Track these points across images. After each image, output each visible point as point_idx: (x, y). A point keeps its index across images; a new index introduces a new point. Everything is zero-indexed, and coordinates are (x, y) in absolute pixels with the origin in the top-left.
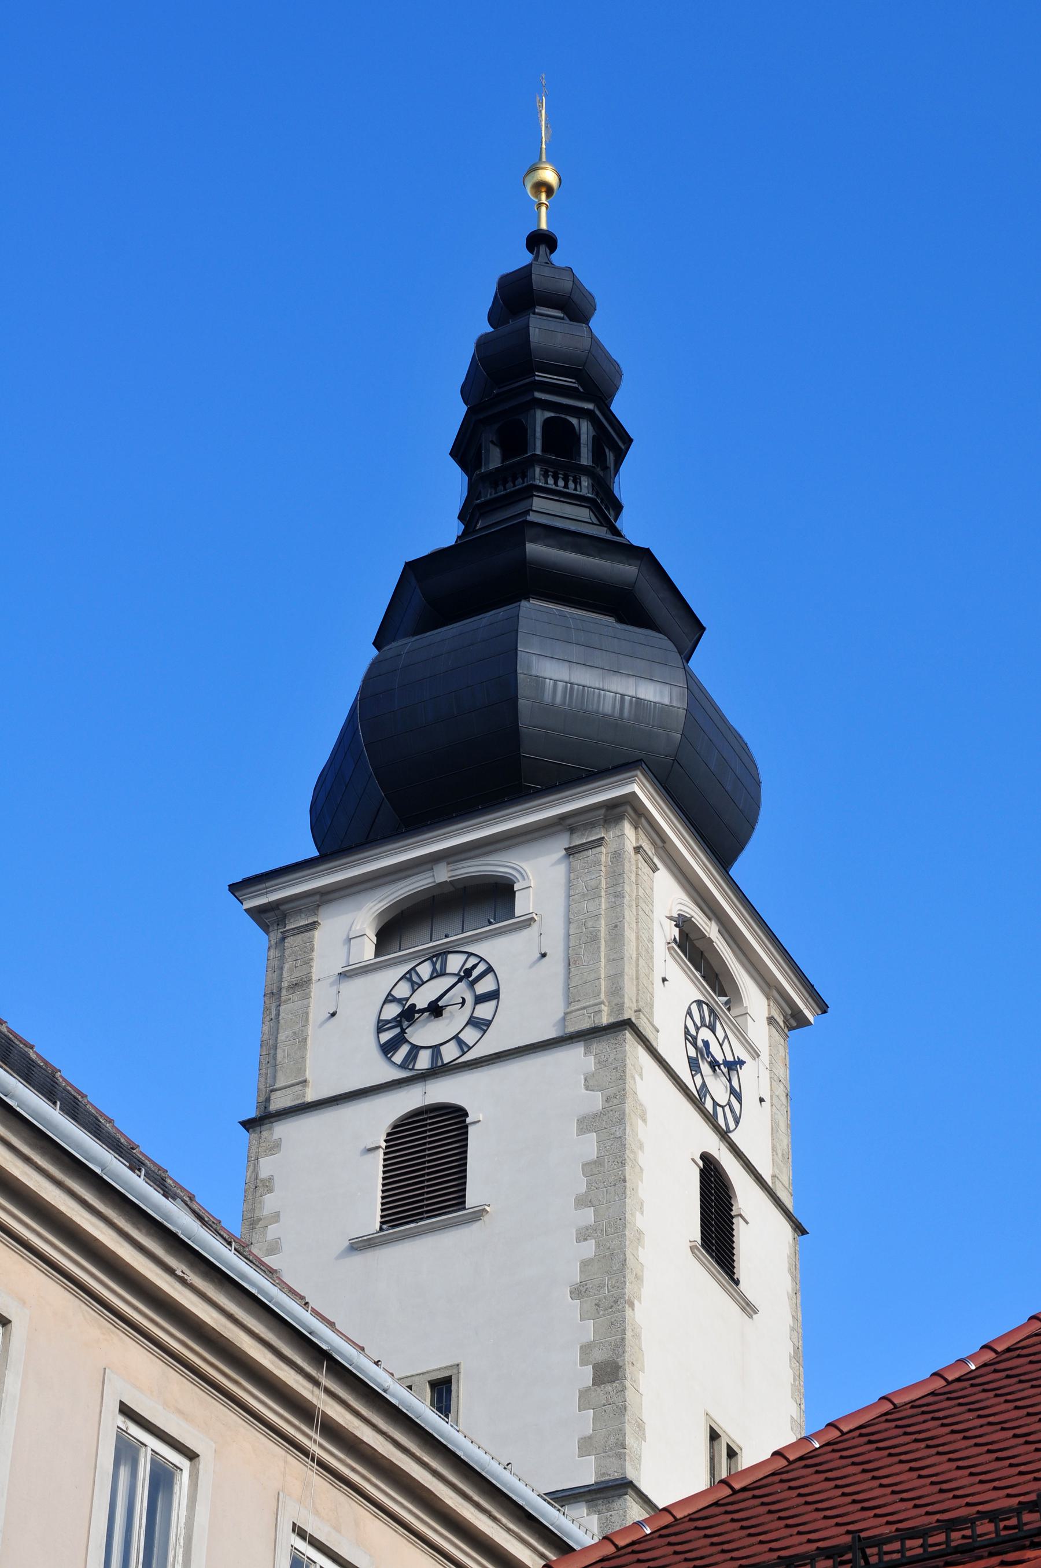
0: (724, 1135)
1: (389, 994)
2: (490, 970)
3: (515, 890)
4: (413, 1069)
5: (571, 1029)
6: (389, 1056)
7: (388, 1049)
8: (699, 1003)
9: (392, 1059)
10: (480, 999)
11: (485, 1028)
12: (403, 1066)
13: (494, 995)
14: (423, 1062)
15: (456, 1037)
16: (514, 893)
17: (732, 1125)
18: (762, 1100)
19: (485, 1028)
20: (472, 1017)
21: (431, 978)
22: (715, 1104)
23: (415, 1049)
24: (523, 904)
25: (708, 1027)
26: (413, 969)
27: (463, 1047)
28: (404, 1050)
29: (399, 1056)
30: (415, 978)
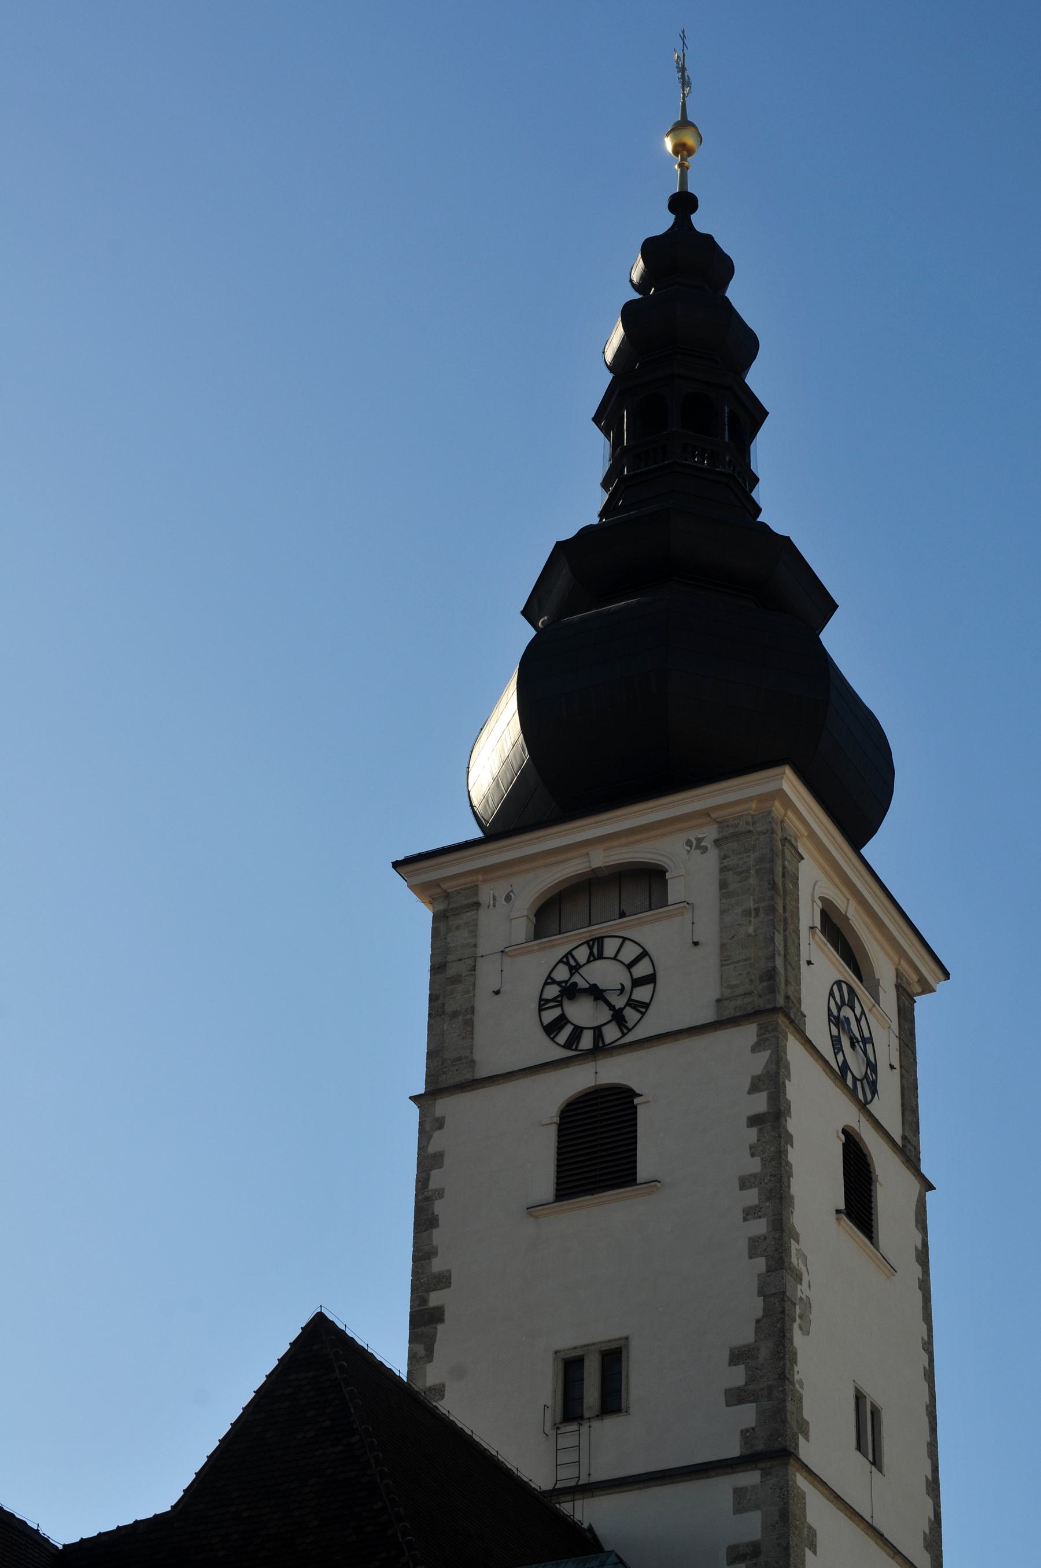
0: (863, 1106)
1: (549, 977)
2: (645, 954)
3: (667, 878)
4: (576, 1049)
5: (727, 1014)
6: (552, 1036)
7: (551, 1029)
8: (839, 983)
9: (556, 1040)
10: (637, 982)
11: (643, 1010)
12: (568, 1045)
13: (650, 979)
14: (586, 1041)
16: (667, 881)
17: (869, 1097)
18: (892, 1067)
19: (643, 1010)
20: (630, 999)
21: (588, 962)
22: (855, 1079)
23: (578, 1032)
24: (675, 891)
25: (848, 1005)
26: (570, 953)
28: (568, 1030)
29: (563, 1037)
30: (573, 963)
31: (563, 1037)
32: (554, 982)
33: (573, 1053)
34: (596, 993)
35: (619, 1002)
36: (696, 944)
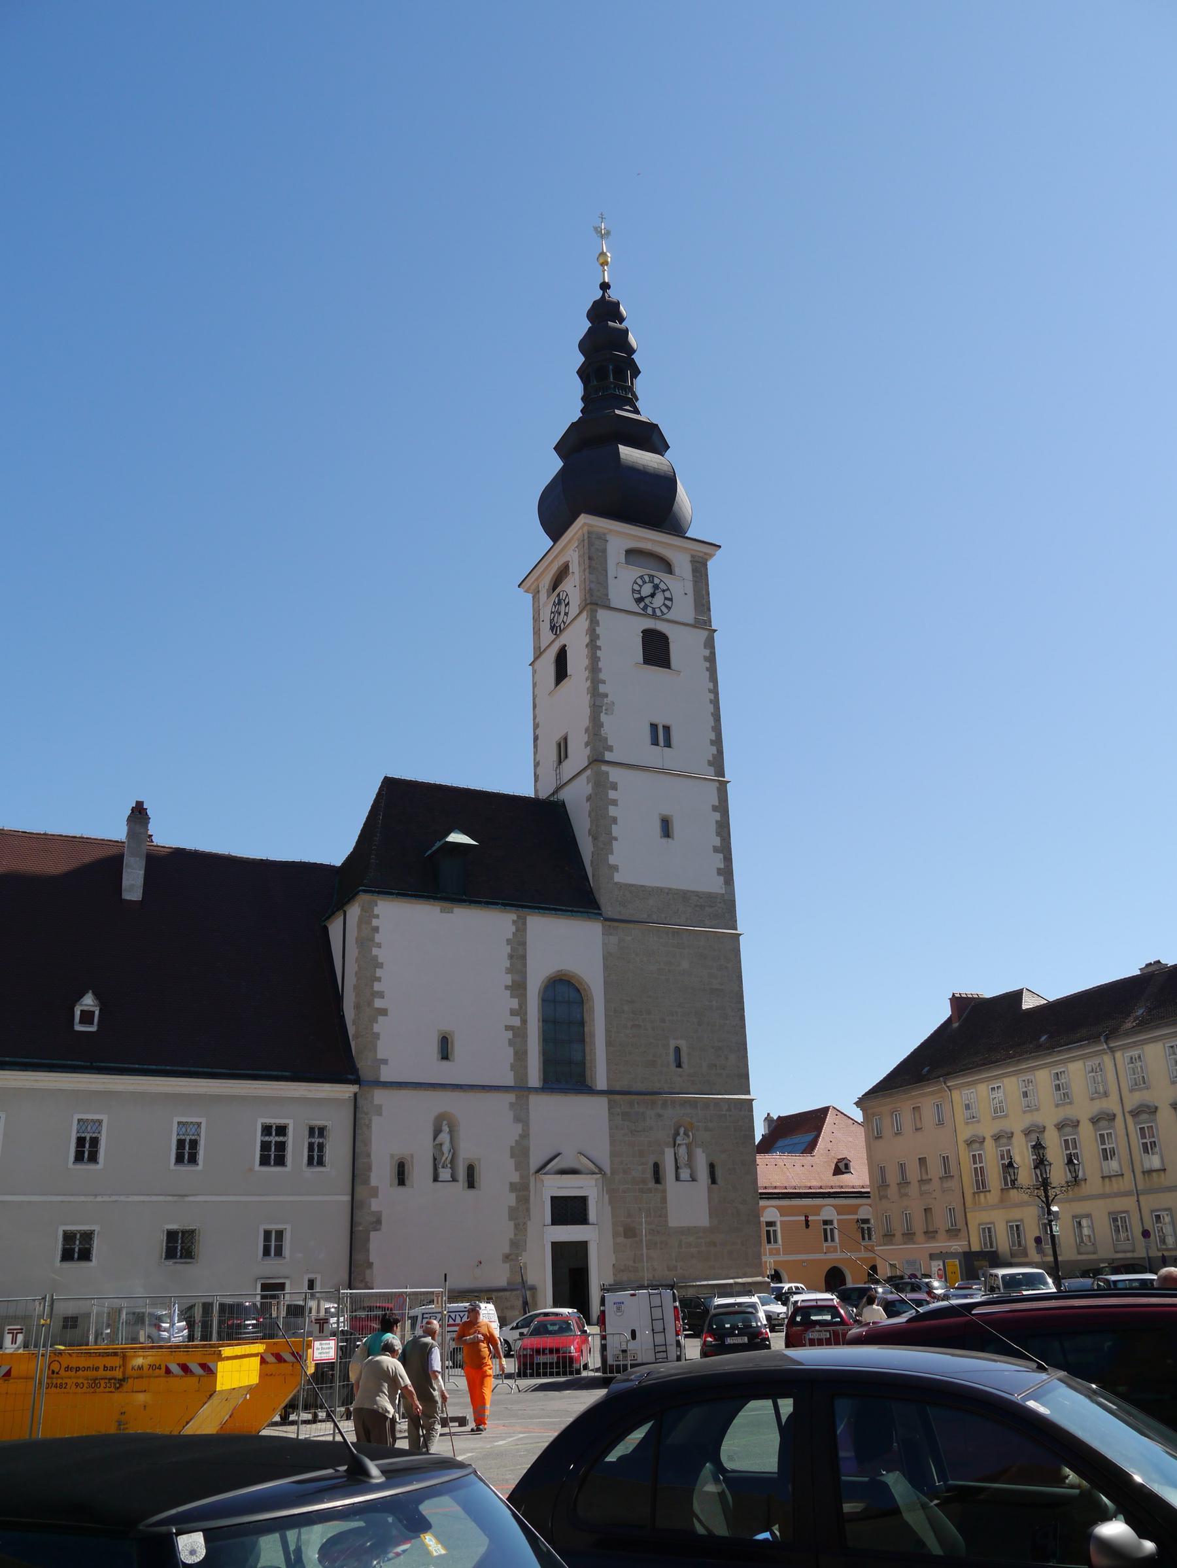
2: (668, 589)
12: (643, 609)
14: (650, 611)
29: (642, 605)
32: (637, 583)
33: (642, 612)
34: (653, 595)
35: (647, 601)
36: (686, 594)
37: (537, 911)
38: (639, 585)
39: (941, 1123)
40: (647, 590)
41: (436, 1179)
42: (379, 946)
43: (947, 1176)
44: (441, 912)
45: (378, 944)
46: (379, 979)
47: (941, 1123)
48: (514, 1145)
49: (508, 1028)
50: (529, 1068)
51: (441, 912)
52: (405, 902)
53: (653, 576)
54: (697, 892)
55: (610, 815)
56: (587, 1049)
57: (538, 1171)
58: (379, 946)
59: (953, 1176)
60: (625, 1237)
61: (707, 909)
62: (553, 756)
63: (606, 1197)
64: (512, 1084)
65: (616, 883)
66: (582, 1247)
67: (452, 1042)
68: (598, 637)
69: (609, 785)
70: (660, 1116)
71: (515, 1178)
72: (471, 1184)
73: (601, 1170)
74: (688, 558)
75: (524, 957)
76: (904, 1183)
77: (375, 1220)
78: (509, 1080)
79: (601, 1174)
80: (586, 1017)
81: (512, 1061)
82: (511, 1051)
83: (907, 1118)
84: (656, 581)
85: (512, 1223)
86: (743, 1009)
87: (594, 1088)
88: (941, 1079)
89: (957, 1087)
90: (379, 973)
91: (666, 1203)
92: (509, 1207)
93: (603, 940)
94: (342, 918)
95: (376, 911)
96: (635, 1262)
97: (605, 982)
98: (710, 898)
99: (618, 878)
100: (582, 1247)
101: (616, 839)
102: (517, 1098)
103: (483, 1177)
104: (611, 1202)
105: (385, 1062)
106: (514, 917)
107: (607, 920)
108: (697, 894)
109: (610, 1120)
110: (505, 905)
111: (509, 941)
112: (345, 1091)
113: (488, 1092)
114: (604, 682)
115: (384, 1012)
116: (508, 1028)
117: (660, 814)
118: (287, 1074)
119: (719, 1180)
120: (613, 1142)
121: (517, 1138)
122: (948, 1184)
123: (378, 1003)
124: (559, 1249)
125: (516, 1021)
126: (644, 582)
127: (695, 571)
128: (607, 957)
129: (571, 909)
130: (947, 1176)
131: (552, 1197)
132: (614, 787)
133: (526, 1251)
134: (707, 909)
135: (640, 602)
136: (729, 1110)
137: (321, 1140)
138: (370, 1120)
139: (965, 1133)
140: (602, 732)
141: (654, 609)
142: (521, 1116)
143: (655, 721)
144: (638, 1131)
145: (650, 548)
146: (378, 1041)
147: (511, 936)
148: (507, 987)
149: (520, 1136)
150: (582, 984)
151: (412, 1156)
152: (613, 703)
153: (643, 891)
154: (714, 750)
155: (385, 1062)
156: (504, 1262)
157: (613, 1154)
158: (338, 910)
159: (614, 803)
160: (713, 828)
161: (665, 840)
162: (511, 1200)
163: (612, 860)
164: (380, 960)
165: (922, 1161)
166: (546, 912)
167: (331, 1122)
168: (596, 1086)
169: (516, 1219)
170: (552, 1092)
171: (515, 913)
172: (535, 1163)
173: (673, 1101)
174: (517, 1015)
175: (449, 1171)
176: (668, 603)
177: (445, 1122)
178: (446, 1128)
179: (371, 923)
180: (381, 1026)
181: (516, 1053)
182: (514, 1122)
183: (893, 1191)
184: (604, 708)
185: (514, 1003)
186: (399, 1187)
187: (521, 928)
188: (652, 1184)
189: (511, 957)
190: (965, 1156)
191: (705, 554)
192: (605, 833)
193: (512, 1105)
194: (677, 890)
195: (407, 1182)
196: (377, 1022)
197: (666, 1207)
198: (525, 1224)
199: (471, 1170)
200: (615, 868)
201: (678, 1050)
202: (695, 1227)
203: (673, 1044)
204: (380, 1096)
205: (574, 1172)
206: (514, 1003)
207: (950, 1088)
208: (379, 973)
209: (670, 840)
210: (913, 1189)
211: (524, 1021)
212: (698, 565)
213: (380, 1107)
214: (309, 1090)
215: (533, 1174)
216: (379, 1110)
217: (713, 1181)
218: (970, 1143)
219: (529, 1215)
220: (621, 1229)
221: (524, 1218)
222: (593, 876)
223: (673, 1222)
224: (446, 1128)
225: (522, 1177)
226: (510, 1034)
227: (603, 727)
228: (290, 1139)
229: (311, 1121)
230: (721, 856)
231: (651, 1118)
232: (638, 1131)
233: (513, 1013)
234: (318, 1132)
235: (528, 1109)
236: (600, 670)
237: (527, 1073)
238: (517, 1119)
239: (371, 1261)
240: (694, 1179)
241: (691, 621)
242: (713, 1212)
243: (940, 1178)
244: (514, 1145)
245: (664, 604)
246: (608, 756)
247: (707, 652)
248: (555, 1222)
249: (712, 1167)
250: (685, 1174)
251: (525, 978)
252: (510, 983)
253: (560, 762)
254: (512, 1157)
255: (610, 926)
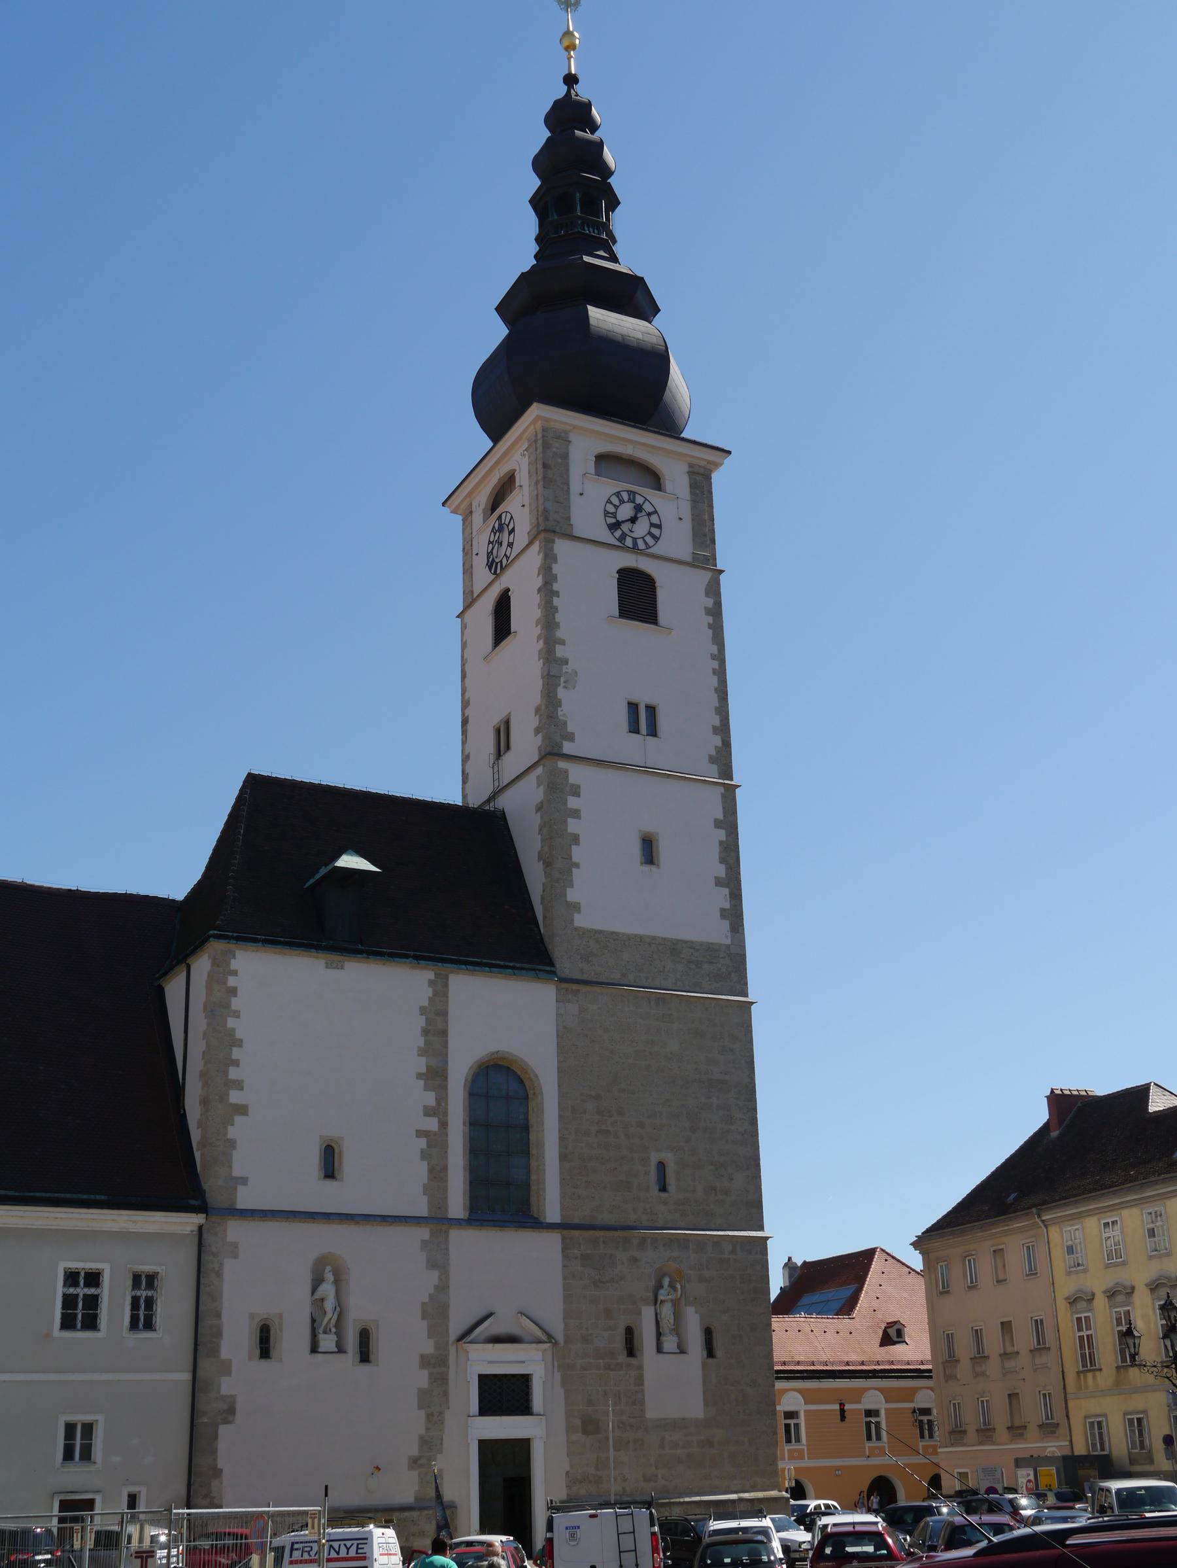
2: (656, 512)
4: (624, 544)
14: (629, 542)
15: (642, 538)
27: (648, 546)
29: (618, 533)
31: (618, 533)
32: (611, 503)
34: (633, 520)
35: (625, 527)
36: (680, 519)
37: (463, 967)
38: (615, 506)
39: (1032, 1273)
40: (625, 512)
41: (314, 1349)
42: (237, 1015)
43: (1041, 1348)
44: (327, 967)
45: (235, 1012)
46: (236, 1063)
47: (1032, 1273)
48: (427, 1300)
49: (420, 1133)
50: (449, 1190)
51: (327, 967)
52: (275, 953)
53: (634, 493)
54: (692, 942)
55: (569, 830)
56: (533, 1164)
57: (460, 1339)
58: (237, 1015)
59: (1049, 1348)
60: (585, 1432)
61: (705, 966)
62: (490, 747)
63: (558, 1376)
64: (424, 1213)
65: (576, 929)
66: (522, 1447)
67: (340, 1153)
68: (555, 578)
69: (568, 789)
70: (635, 1260)
71: (429, 1347)
72: (365, 1356)
73: (550, 1338)
74: (685, 468)
75: (444, 1033)
76: (980, 1358)
77: (225, 1407)
78: (421, 1208)
79: (551, 1342)
80: (532, 1120)
81: (426, 1182)
82: (424, 1167)
83: (985, 1267)
84: (639, 500)
85: (422, 1413)
86: (755, 1110)
87: (542, 1219)
88: (1034, 1210)
89: (1058, 1222)
90: (236, 1053)
91: (642, 1384)
92: (419, 1389)
93: (558, 1009)
94: (184, 974)
95: (234, 964)
96: (597, 1469)
97: (560, 1070)
98: (710, 951)
99: (580, 921)
100: (522, 1447)
101: (577, 866)
102: (431, 1234)
103: (382, 1346)
104: (564, 1383)
105: (244, 1181)
106: (430, 975)
107: (563, 980)
108: (692, 945)
109: (564, 1266)
110: (417, 958)
111: (423, 1010)
112: (185, 1223)
113: (391, 1225)
114: (563, 642)
115: (242, 1110)
116: (420, 1133)
117: (640, 831)
118: (103, 1197)
119: (719, 1351)
120: (567, 1298)
121: (432, 1291)
122: (1041, 1359)
123: (235, 1097)
124: (488, 1448)
125: (432, 1124)
126: (622, 502)
127: (694, 486)
128: (563, 1033)
129: (511, 964)
130: (1041, 1348)
131: (480, 1376)
132: (576, 791)
133: (441, 1453)
134: (705, 966)
135: (616, 530)
136: (733, 1252)
137: (150, 1293)
138: (222, 1264)
139: (1066, 1287)
140: (560, 713)
141: (635, 540)
142: (438, 1262)
143: (634, 699)
144: (603, 1282)
145: (631, 454)
146: (234, 1153)
147: (426, 1004)
148: (419, 1076)
149: (437, 1288)
150: (526, 1073)
151: (281, 1316)
152: (576, 672)
153: (614, 940)
154: (718, 740)
155: (244, 1181)
156: (411, 1468)
157: (567, 1315)
158: (179, 962)
159: (576, 814)
160: (716, 851)
161: (647, 868)
162: (422, 1378)
163: (572, 895)
164: (238, 1035)
165: (1006, 1326)
166: (477, 968)
167: (164, 1267)
168: (545, 1218)
169: (429, 1407)
170: (482, 1225)
171: (433, 970)
172: (455, 1329)
173: (655, 1241)
174: (434, 1115)
175: (334, 1337)
176: (656, 531)
177: (328, 1268)
178: (329, 1277)
179: (225, 983)
180: (238, 1130)
181: (431, 1170)
182: (427, 1268)
183: (964, 1369)
184: (562, 679)
185: (430, 1099)
186: (262, 1360)
187: (440, 993)
188: (622, 1358)
189: (425, 1032)
190: (1066, 1318)
191: (709, 462)
192: (562, 858)
193: (424, 1243)
194: (662, 938)
195: (273, 1353)
196: (233, 1125)
197: (643, 1391)
198: (441, 1413)
199: (365, 1337)
200: (576, 907)
201: (661, 1166)
202: (683, 1419)
203: (654, 1158)
204: (235, 1230)
205: (512, 1339)
206: (430, 1099)
207: (1046, 1223)
208: (236, 1053)
209: (654, 868)
210: (993, 1366)
211: (444, 1125)
212: (698, 478)
213: (235, 1246)
214: (134, 1222)
215: (453, 1343)
216: (234, 1250)
217: (710, 1353)
218: (1073, 1301)
219: (447, 1401)
220: (578, 1422)
221: (441, 1405)
222: (545, 917)
223: (651, 1414)
224: (329, 1277)
225: (437, 1348)
226: (423, 1143)
227: (560, 706)
228: (105, 1292)
229: (137, 1266)
230: (726, 891)
231: (623, 1263)
232: (603, 1282)
233: (428, 1112)
234: (145, 1281)
235: (447, 1249)
236: (557, 625)
237: (446, 1198)
238: (432, 1264)
239: (220, 1466)
240: (682, 1351)
241: (688, 558)
242: (710, 1398)
243: (1031, 1351)
244: (427, 1300)
245: (650, 533)
246: (568, 748)
247: (709, 602)
248: (483, 1411)
249: (708, 1334)
250: (670, 1343)
251: (446, 1063)
252: (424, 1070)
253: (499, 755)
254: (423, 1318)
255: (567, 989)
